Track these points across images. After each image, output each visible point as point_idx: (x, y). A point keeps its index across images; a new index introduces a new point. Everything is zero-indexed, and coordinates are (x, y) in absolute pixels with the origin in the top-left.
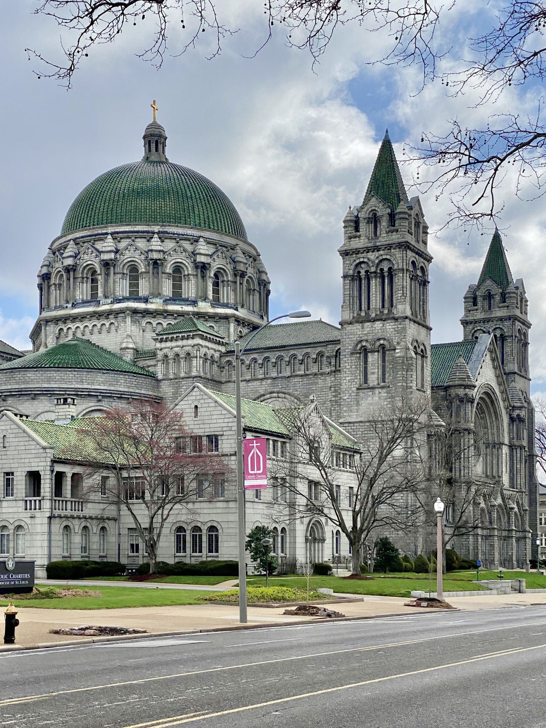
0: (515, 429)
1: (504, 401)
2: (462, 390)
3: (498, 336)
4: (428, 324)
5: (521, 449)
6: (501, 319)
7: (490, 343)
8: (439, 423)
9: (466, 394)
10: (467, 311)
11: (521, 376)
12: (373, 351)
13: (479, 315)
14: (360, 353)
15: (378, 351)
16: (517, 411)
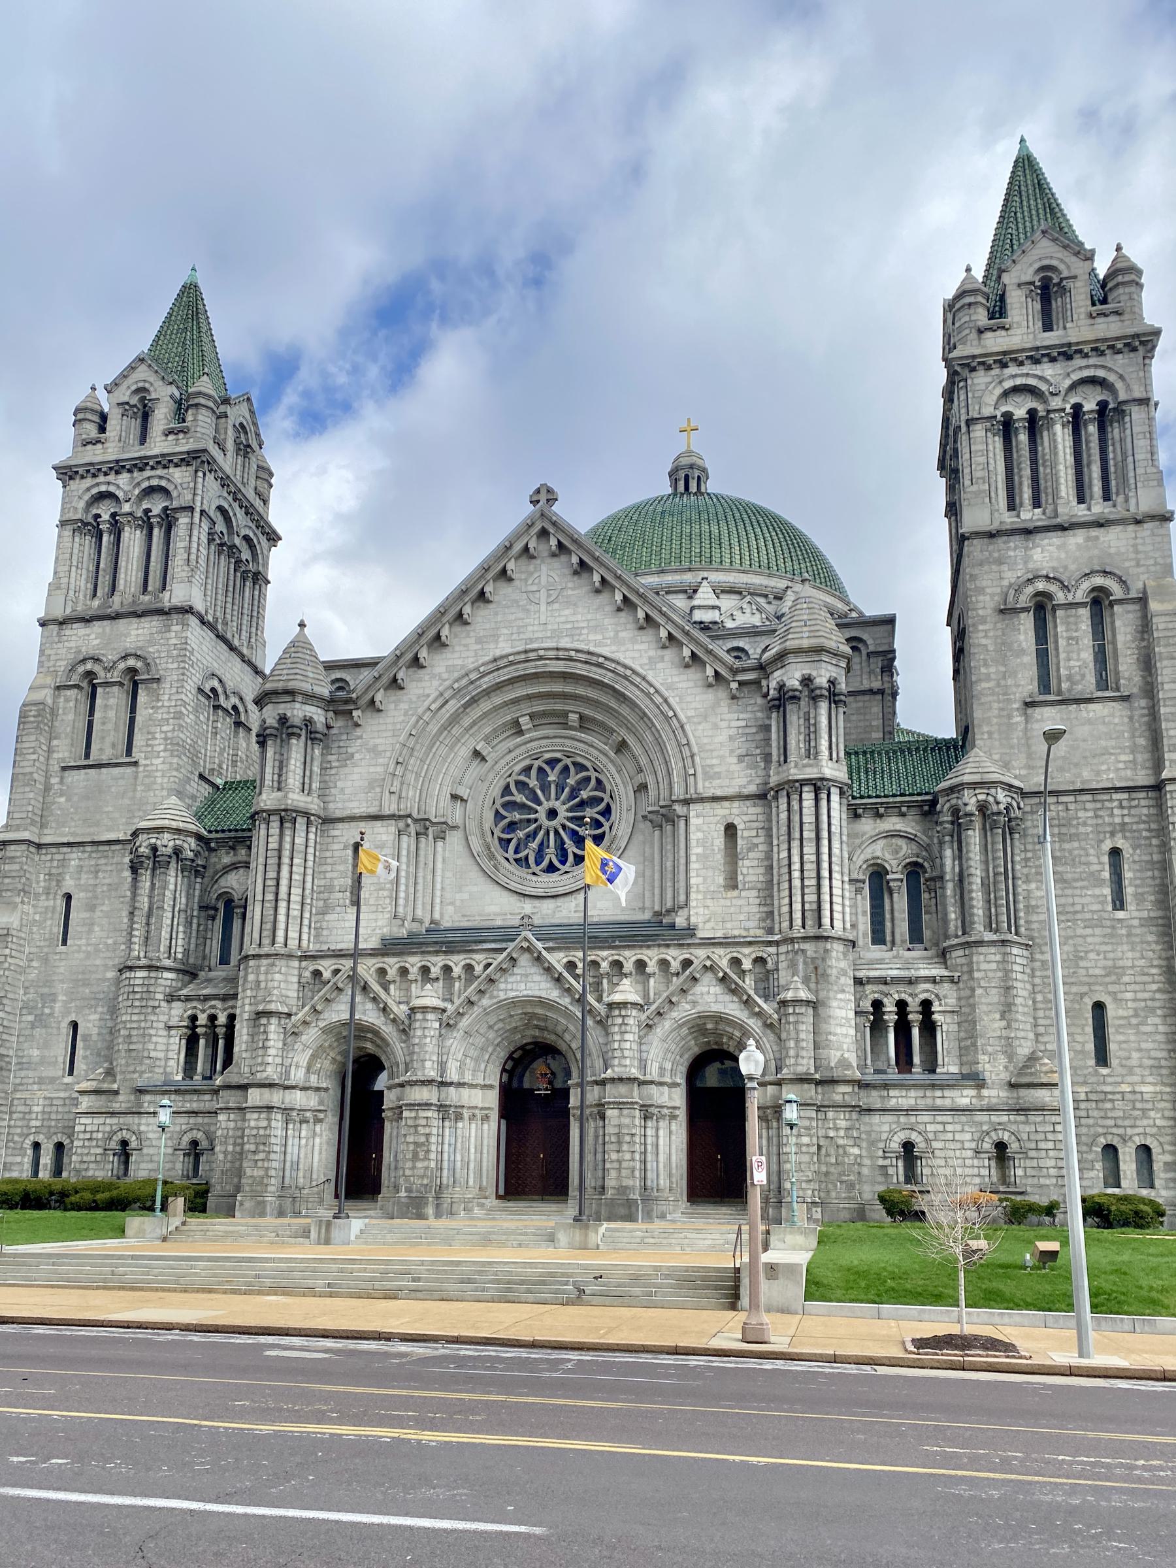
16: (776, 674)
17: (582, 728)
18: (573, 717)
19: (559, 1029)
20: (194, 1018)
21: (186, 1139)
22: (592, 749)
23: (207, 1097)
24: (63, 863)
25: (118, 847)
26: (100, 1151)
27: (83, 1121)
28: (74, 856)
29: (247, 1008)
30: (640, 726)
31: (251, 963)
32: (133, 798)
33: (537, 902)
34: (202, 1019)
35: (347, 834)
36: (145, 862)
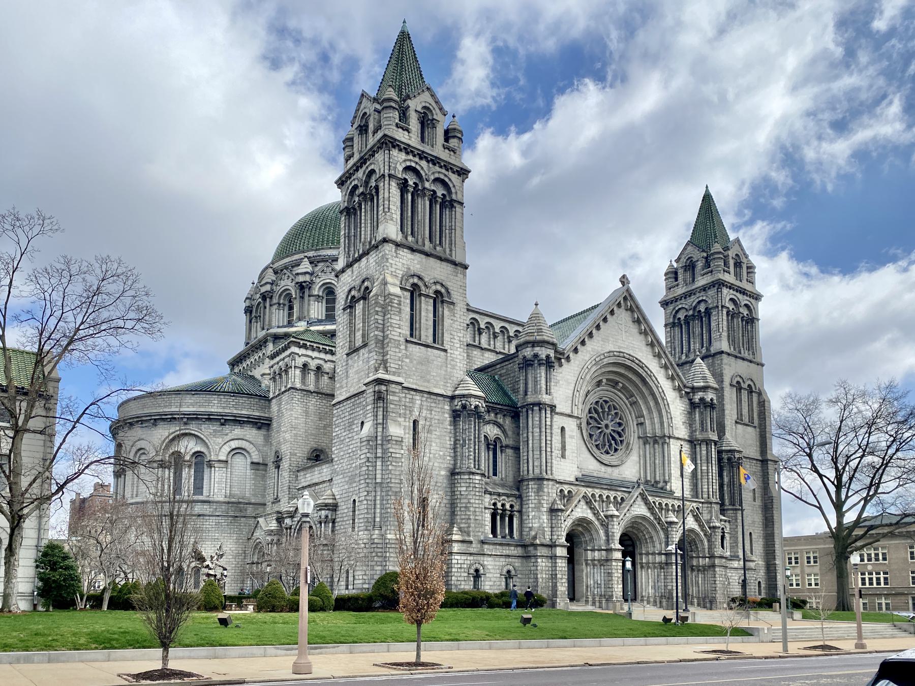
0: (697, 418)
1: (672, 379)
2: (528, 349)
3: (703, 310)
4: (458, 259)
5: (707, 444)
6: (704, 289)
7: (625, 299)
8: (466, 392)
9: (536, 356)
10: (669, 289)
11: (736, 357)
12: (359, 300)
13: (680, 291)
14: (351, 307)
15: (364, 298)
17: (619, 390)
18: (621, 385)
19: (643, 528)
20: (495, 504)
21: (505, 570)
22: (621, 400)
23: (512, 548)
24: (412, 401)
25: (441, 398)
26: (466, 574)
27: (456, 557)
28: (418, 398)
29: (545, 505)
30: (650, 398)
31: (545, 482)
32: (446, 371)
33: (606, 468)
34: (499, 506)
35: (559, 421)
36: (461, 412)
